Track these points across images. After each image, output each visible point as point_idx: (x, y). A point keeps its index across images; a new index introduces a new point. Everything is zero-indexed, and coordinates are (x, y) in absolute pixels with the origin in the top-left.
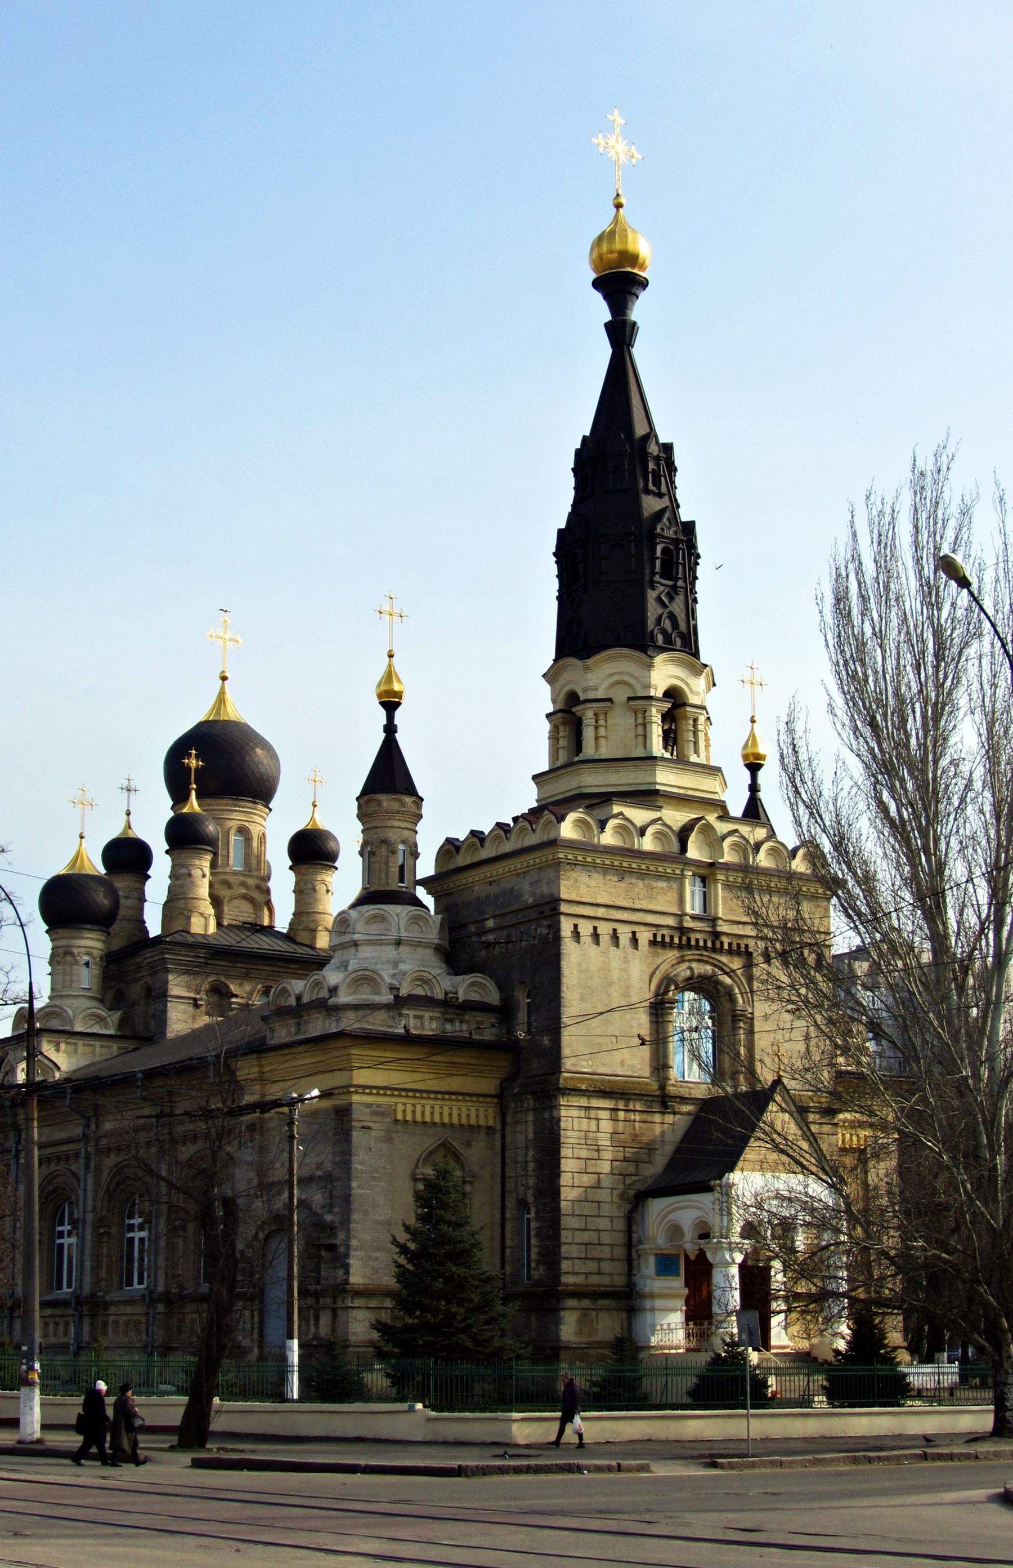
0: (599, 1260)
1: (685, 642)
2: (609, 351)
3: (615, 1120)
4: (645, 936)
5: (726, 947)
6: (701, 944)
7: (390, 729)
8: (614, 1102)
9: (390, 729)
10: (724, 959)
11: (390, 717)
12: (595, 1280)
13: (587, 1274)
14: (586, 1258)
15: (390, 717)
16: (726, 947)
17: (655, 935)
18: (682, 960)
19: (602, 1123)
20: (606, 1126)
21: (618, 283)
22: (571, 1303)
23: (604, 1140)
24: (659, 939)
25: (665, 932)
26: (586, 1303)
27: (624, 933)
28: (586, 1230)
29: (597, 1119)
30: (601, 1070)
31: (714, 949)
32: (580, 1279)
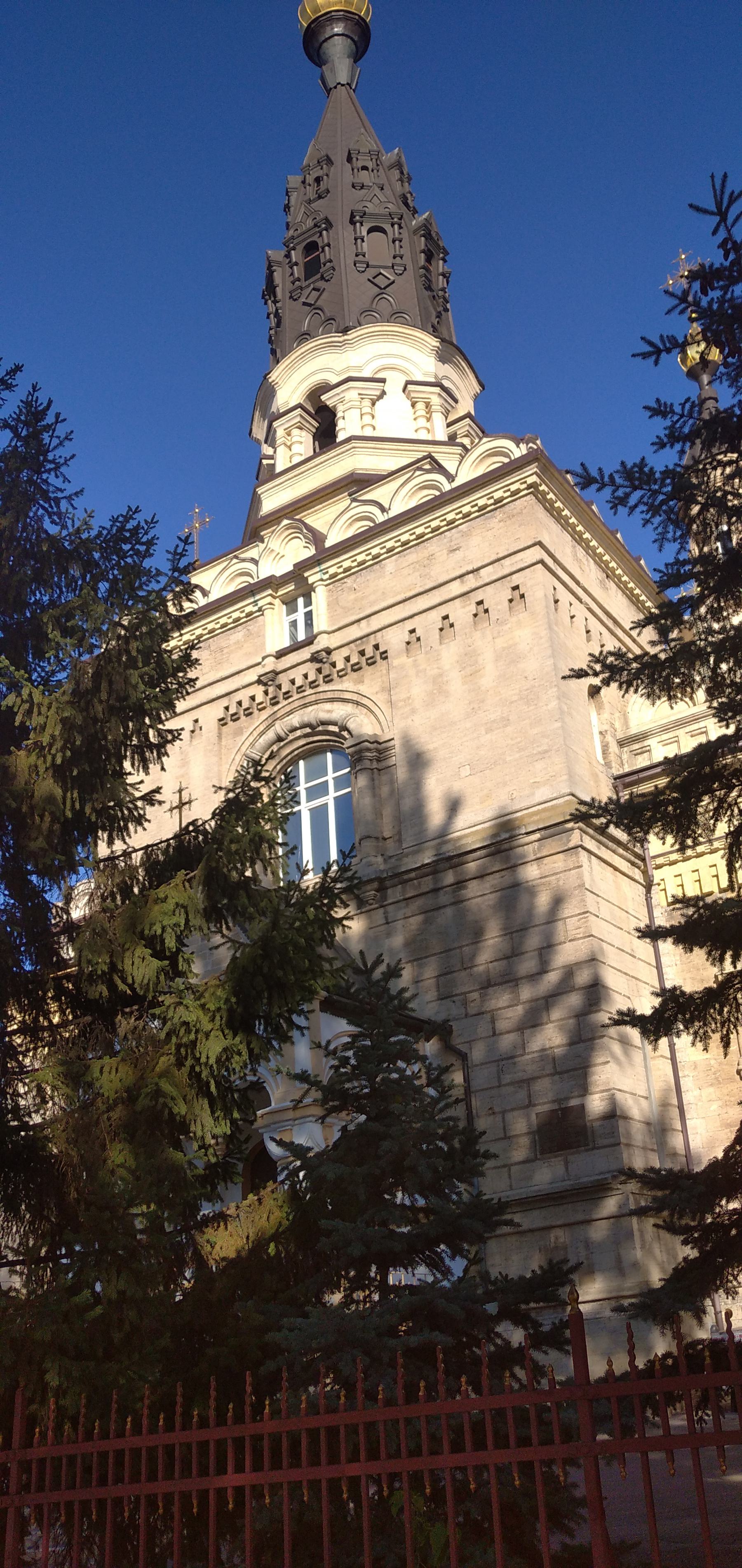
5: (340, 665)
10: (347, 684)
18: (273, 720)
31: (328, 680)
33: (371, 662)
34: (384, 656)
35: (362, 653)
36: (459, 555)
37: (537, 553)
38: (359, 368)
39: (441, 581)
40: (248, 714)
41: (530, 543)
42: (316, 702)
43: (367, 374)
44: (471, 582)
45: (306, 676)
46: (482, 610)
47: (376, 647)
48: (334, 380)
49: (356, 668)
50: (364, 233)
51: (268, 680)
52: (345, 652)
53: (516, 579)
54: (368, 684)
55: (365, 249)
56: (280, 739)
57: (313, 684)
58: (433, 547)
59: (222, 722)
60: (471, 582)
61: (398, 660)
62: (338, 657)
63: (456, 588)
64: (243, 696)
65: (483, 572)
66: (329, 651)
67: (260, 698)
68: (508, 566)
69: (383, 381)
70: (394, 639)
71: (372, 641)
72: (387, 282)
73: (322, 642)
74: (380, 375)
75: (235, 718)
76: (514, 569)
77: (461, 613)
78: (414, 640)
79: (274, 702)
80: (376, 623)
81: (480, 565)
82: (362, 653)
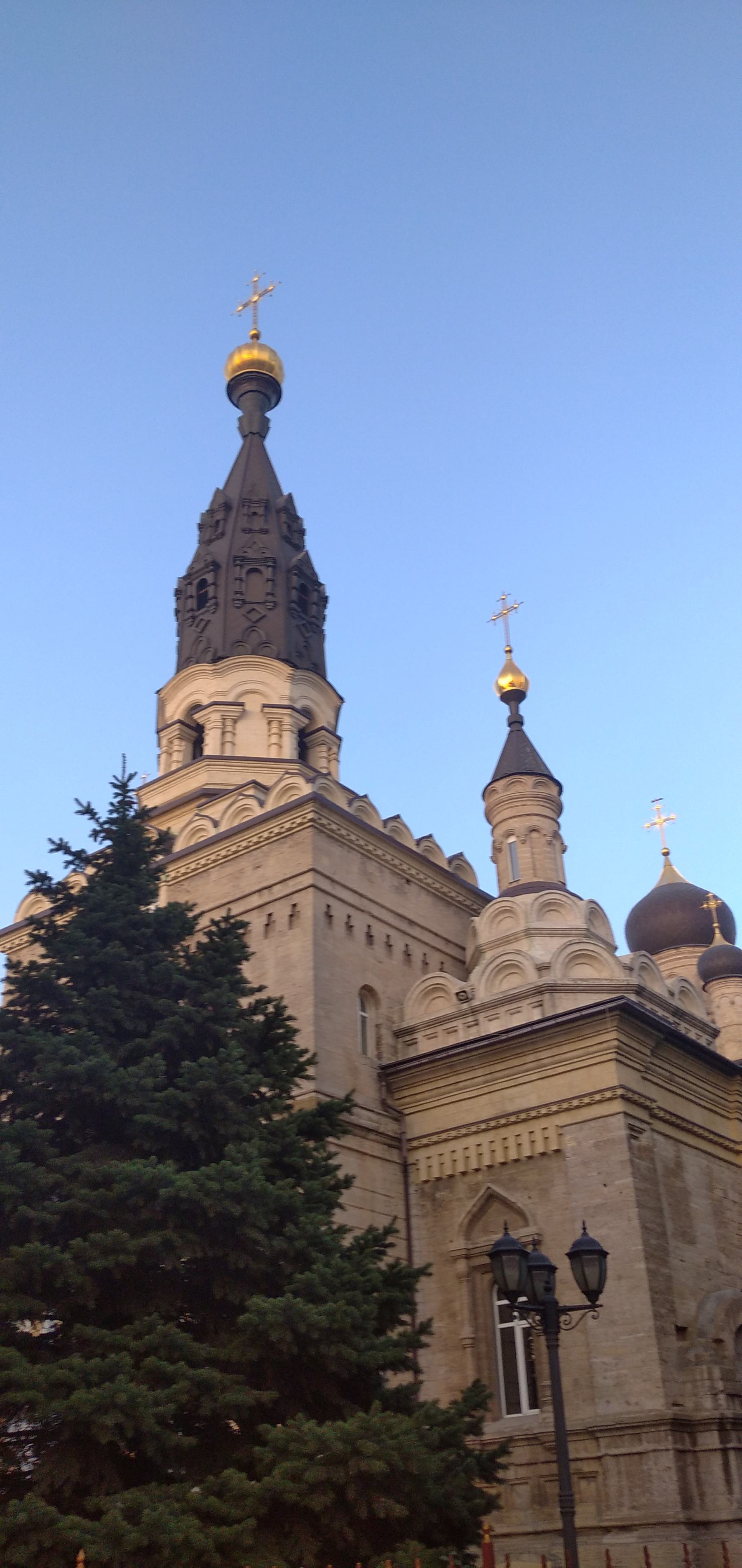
36: (260, 871)
37: (308, 879)
38: (224, 693)
39: (247, 892)
41: (306, 869)
43: (230, 699)
44: (266, 897)
48: (205, 702)
50: (243, 576)
53: (296, 899)
55: (243, 590)
58: (245, 863)
60: (266, 897)
65: (275, 888)
68: (292, 886)
69: (242, 704)
72: (259, 616)
74: (241, 700)
76: (294, 890)
81: (273, 882)
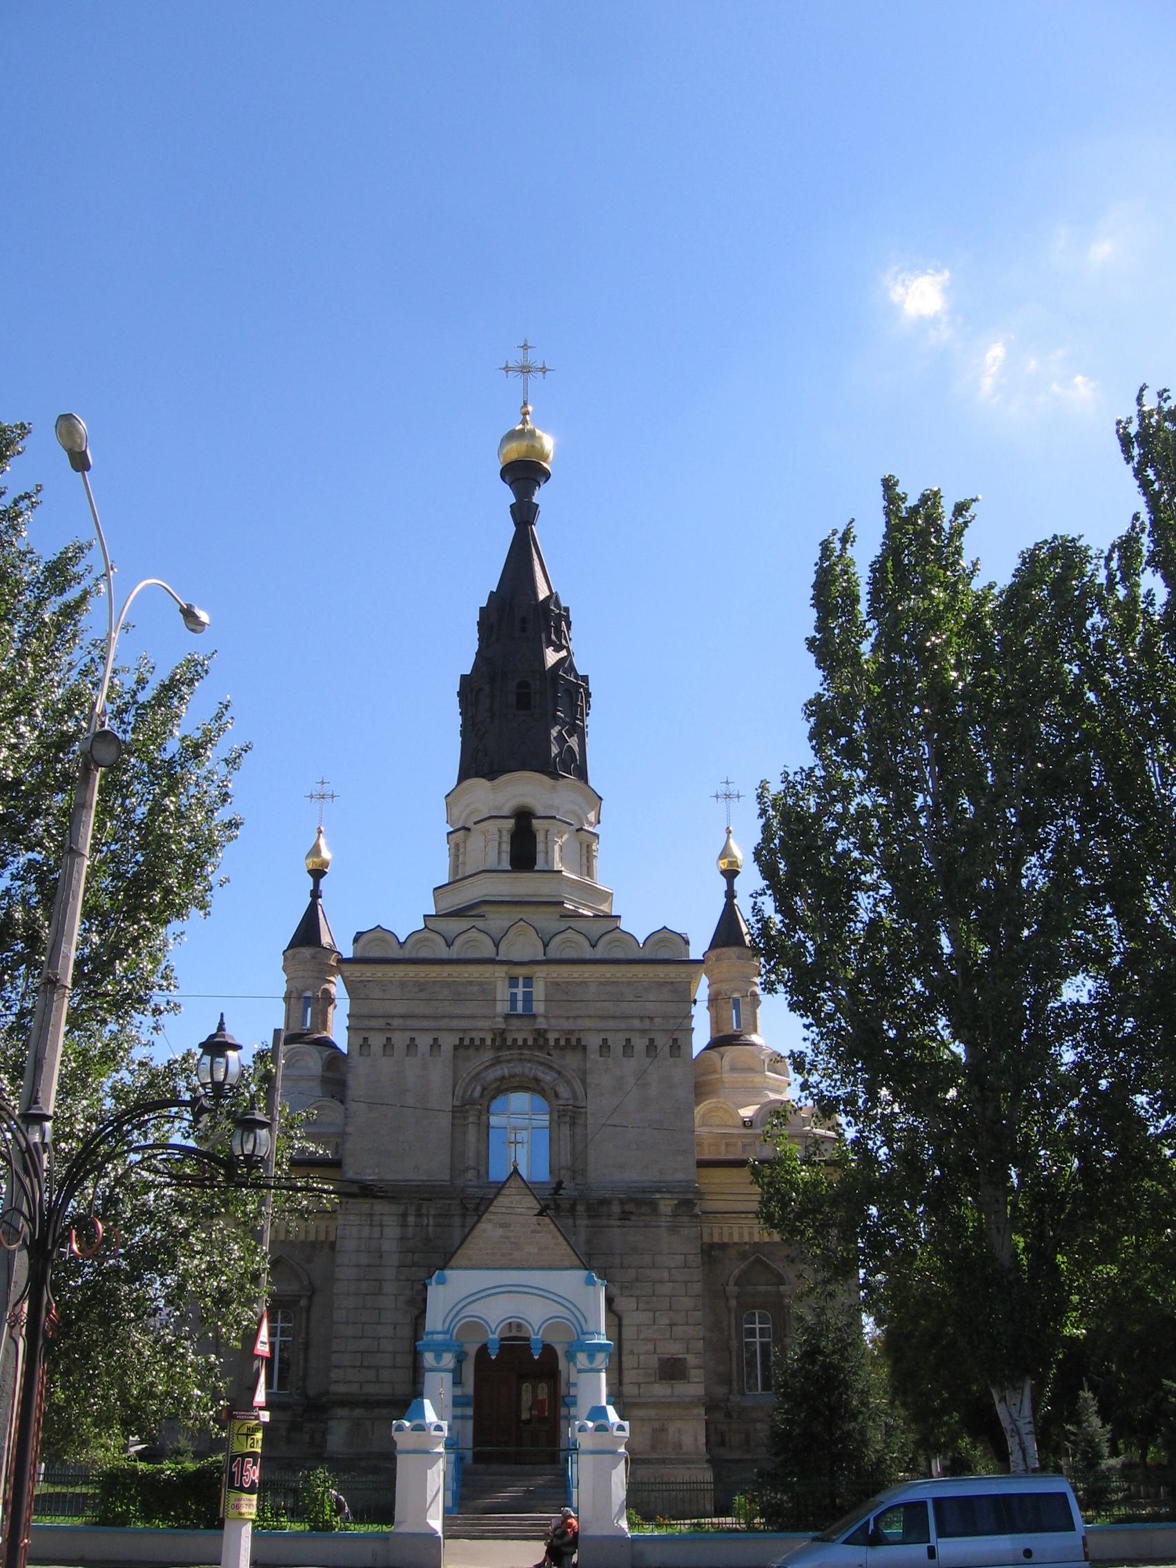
0: (377, 1368)
1: (575, 766)
2: (512, 529)
3: (404, 1225)
4: (448, 1041)
5: (552, 1043)
6: (520, 1042)
7: (316, 894)
8: (403, 1207)
9: (316, 894)
11: (316, 884)
12: (371, 1389)
13: (361, 1383)
14: (361, 1366)
15: (316, 884)
16: (552, 1043)
17: (461, 1040)
18: (497, 1061)
19: (387, 1231)
20: (392, 1231)
21: (524, 474)
22: (340, 1412)
23: (389, 1246)
24: (466, 1042)
25: (473, 1034)
26: (359, 1412)
27: (424, 1041)
28: (362, 1337)
29: (381, 1226)
30: (389, 1177)
31: (541, 1048)
32: (354, 1388)
33: (574, 1048)
34: (585, 1048)
35: (568, 1040)
40: (477, 1048)
42: (530, 1061)
44: (647, 1024)
45: (525, 1040)
46: (652, 1047)
47: (579, 1040)
49: (563, 1049)
51: (500, 1035)
52: (556, 1035)
54: (571, 1061)
56: (503, 1079)
57: (530, 1048)
59: (456, 1048)
61: (594, 1056)
62: (552, 1037)
63: (636, 1023)
64: (477, 1036)
66: (546, 1031)
67: (489, 1042)
70: (593, 1041)
71: (577, 1035)
73: (541, 1023)
75: (467, 1047)
77: (640, 1043)
78: (605, 1047)
79: (499, 1049)
80: (581, 1024)
82: (568, 1040)
